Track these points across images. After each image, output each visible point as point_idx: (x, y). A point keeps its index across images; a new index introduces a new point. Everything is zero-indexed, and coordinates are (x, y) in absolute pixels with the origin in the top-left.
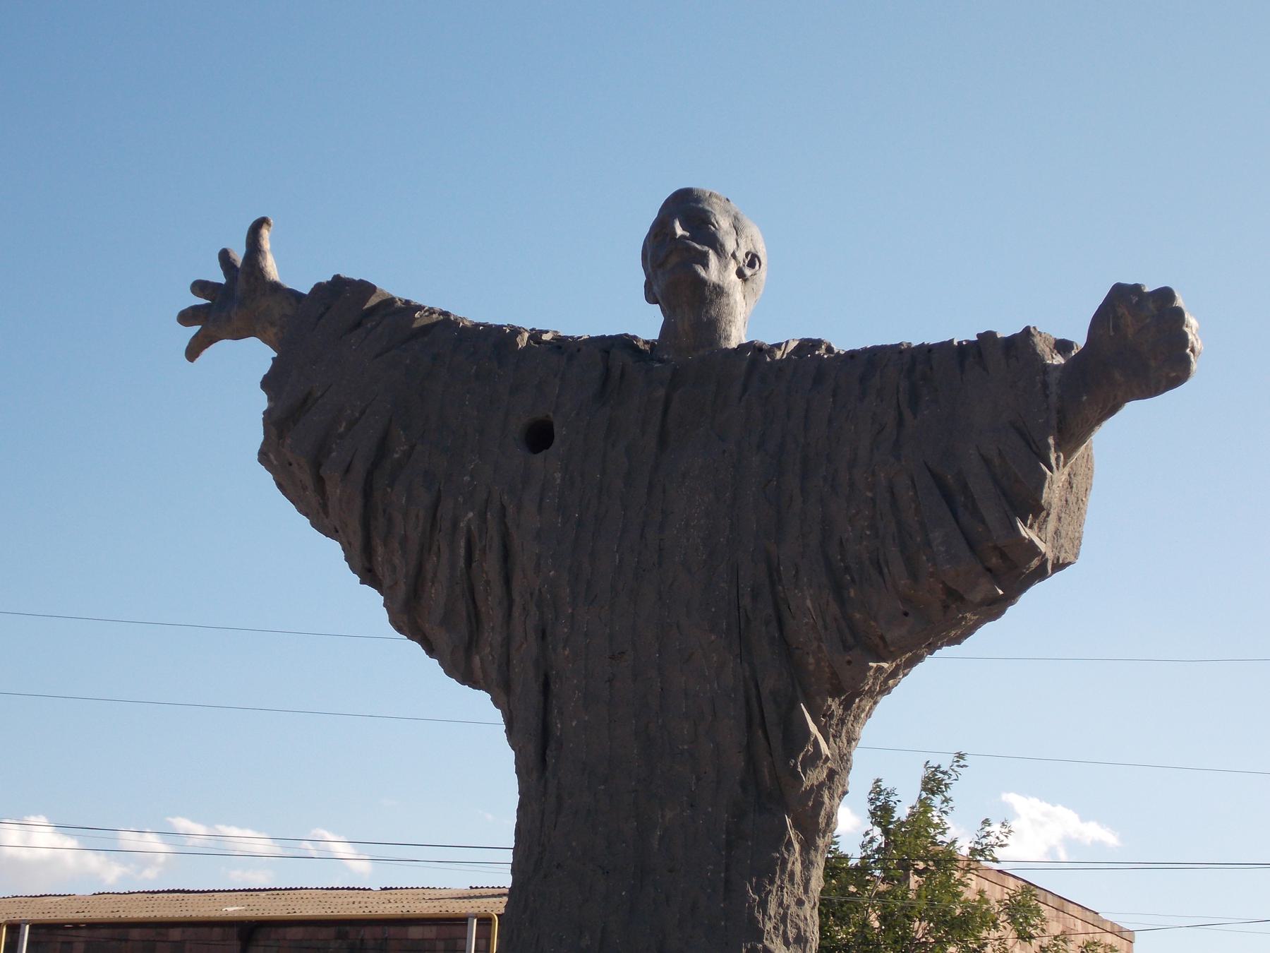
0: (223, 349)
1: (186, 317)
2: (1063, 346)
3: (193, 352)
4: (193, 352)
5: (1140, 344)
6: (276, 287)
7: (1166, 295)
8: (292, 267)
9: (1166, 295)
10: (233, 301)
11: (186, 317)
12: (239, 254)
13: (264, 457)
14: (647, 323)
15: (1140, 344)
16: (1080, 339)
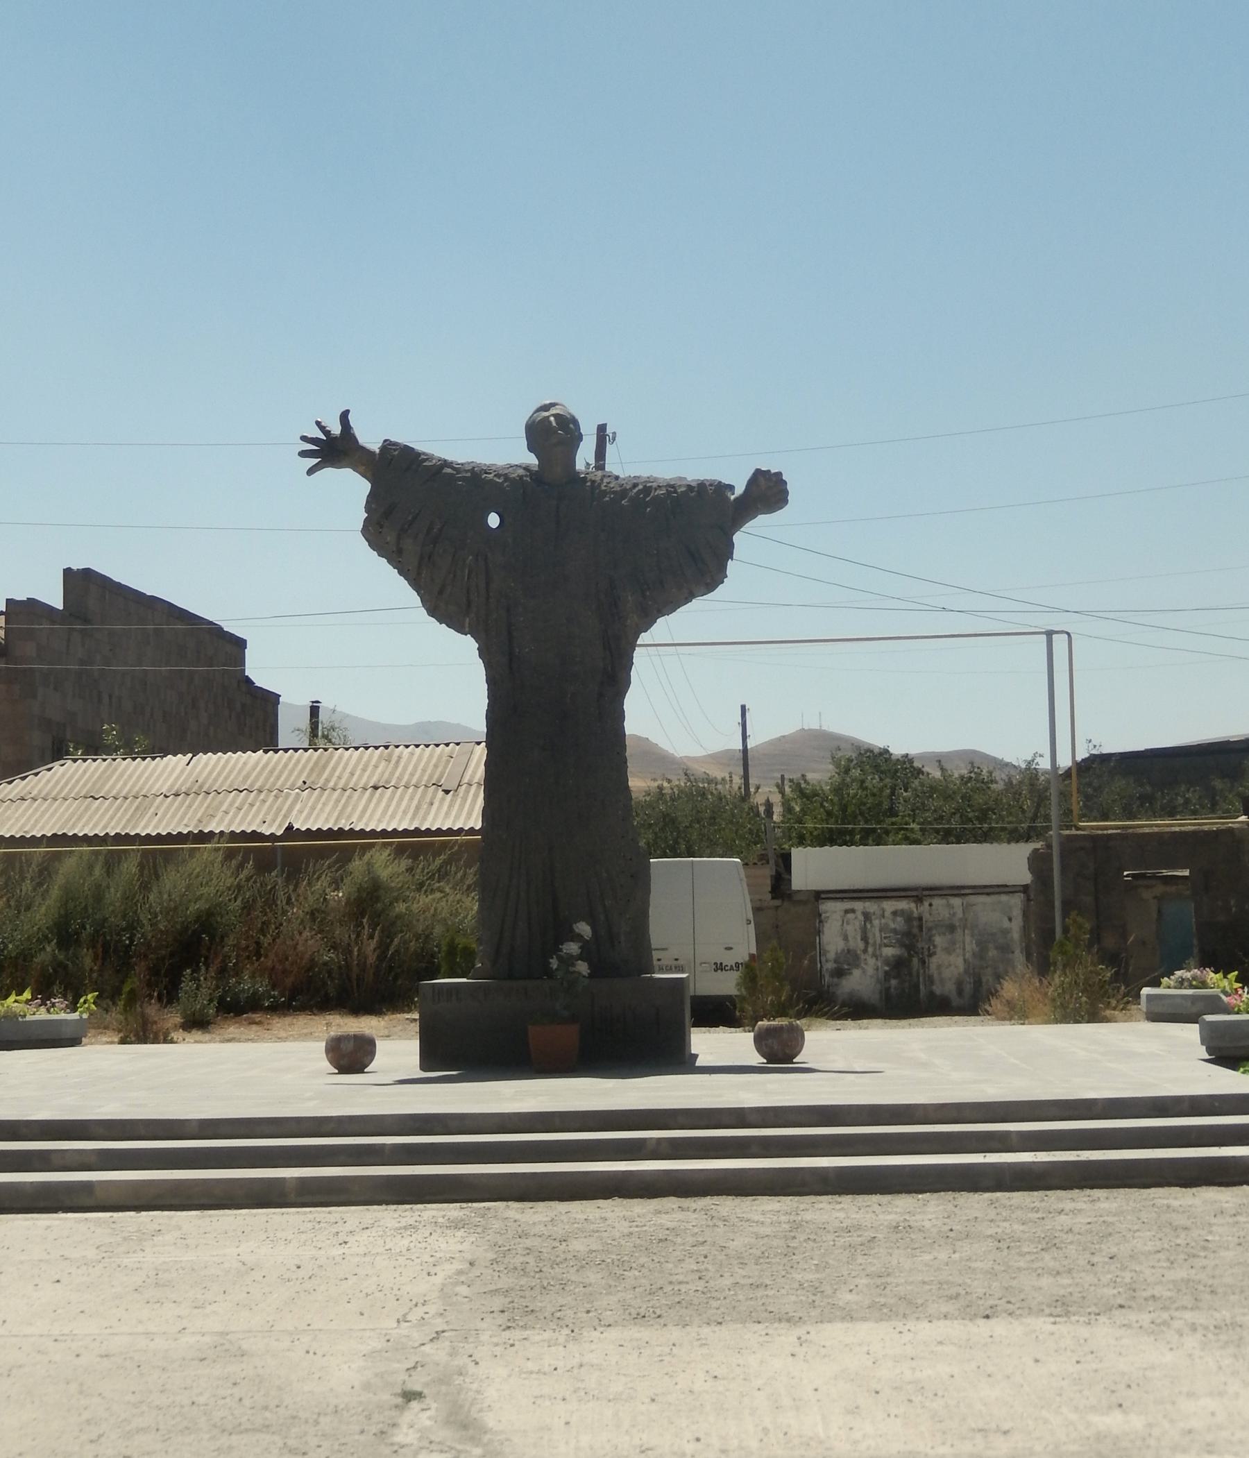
0: (328, 472)
1: (304, 454)
2: (731, 488)
3: (311, 471)
4: (311, 471)
5: (767, 492)
6: (363, 448)
7: (779, 474)
8: (370, 438)
9: (779, 474)
10: (334, 449)
11: (304, 454)
12: (336, 429)
13: (366, 531)
14: (532, 460)
15: (767, 492)
16: (740, 490)
